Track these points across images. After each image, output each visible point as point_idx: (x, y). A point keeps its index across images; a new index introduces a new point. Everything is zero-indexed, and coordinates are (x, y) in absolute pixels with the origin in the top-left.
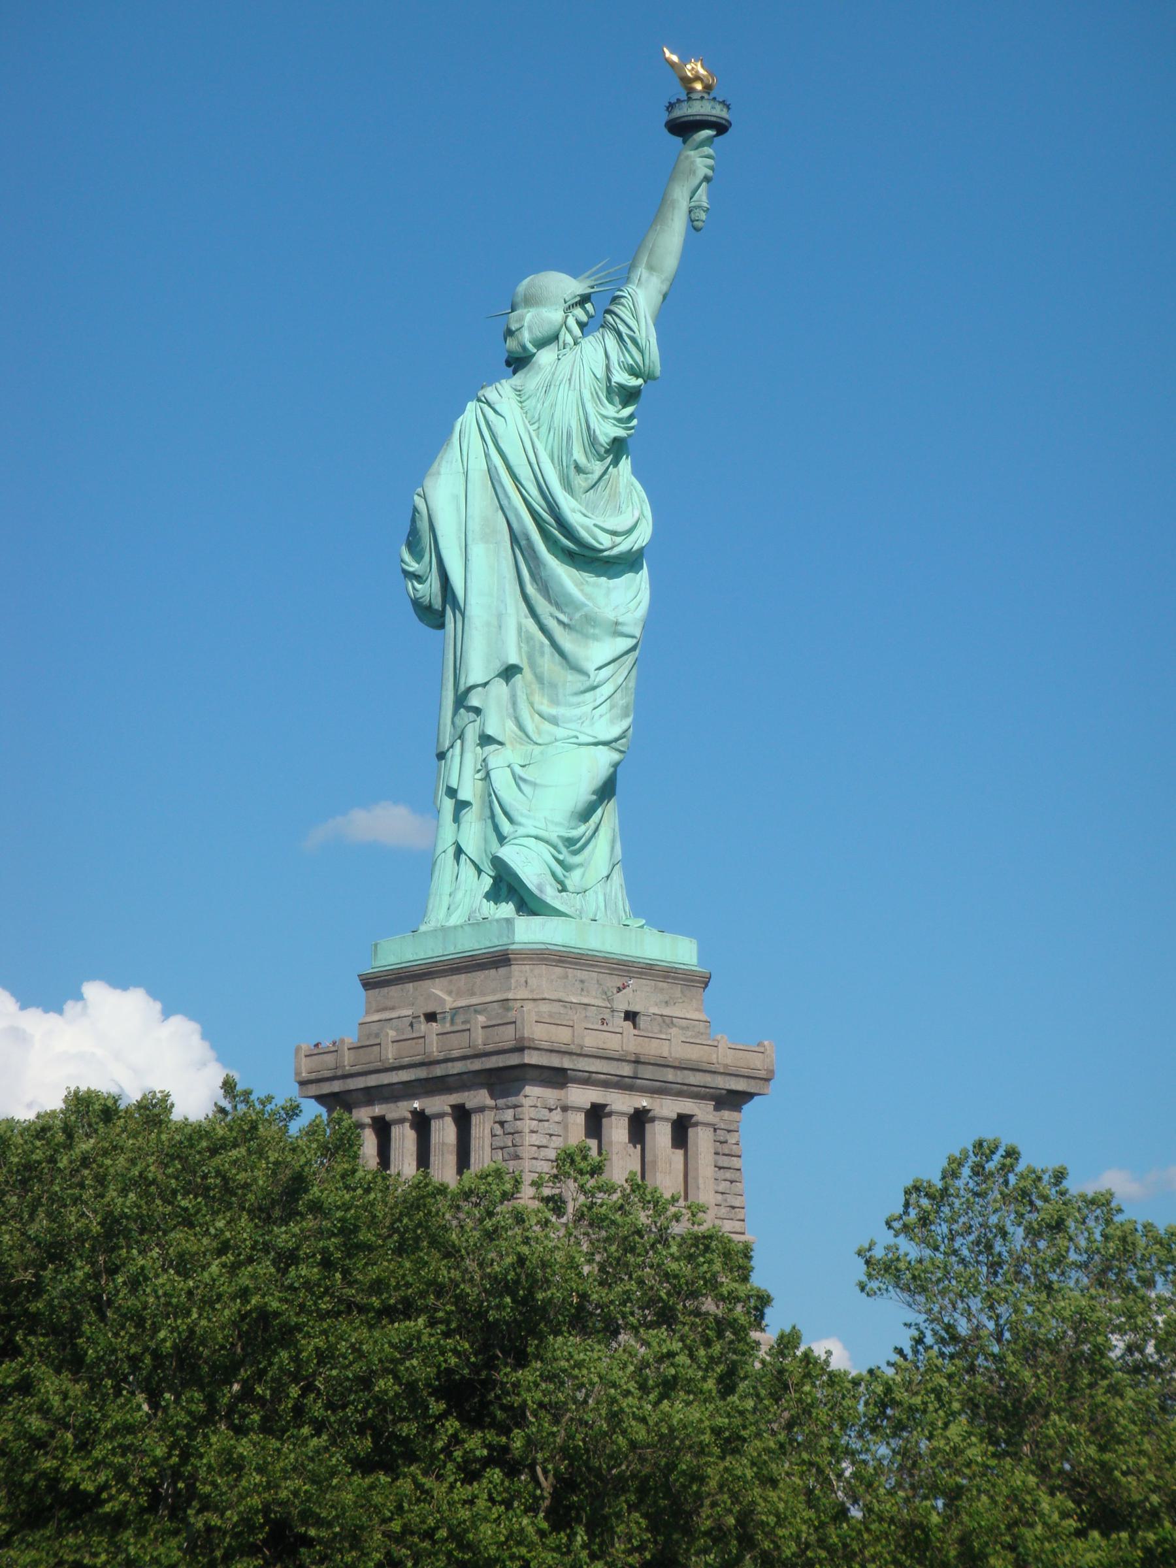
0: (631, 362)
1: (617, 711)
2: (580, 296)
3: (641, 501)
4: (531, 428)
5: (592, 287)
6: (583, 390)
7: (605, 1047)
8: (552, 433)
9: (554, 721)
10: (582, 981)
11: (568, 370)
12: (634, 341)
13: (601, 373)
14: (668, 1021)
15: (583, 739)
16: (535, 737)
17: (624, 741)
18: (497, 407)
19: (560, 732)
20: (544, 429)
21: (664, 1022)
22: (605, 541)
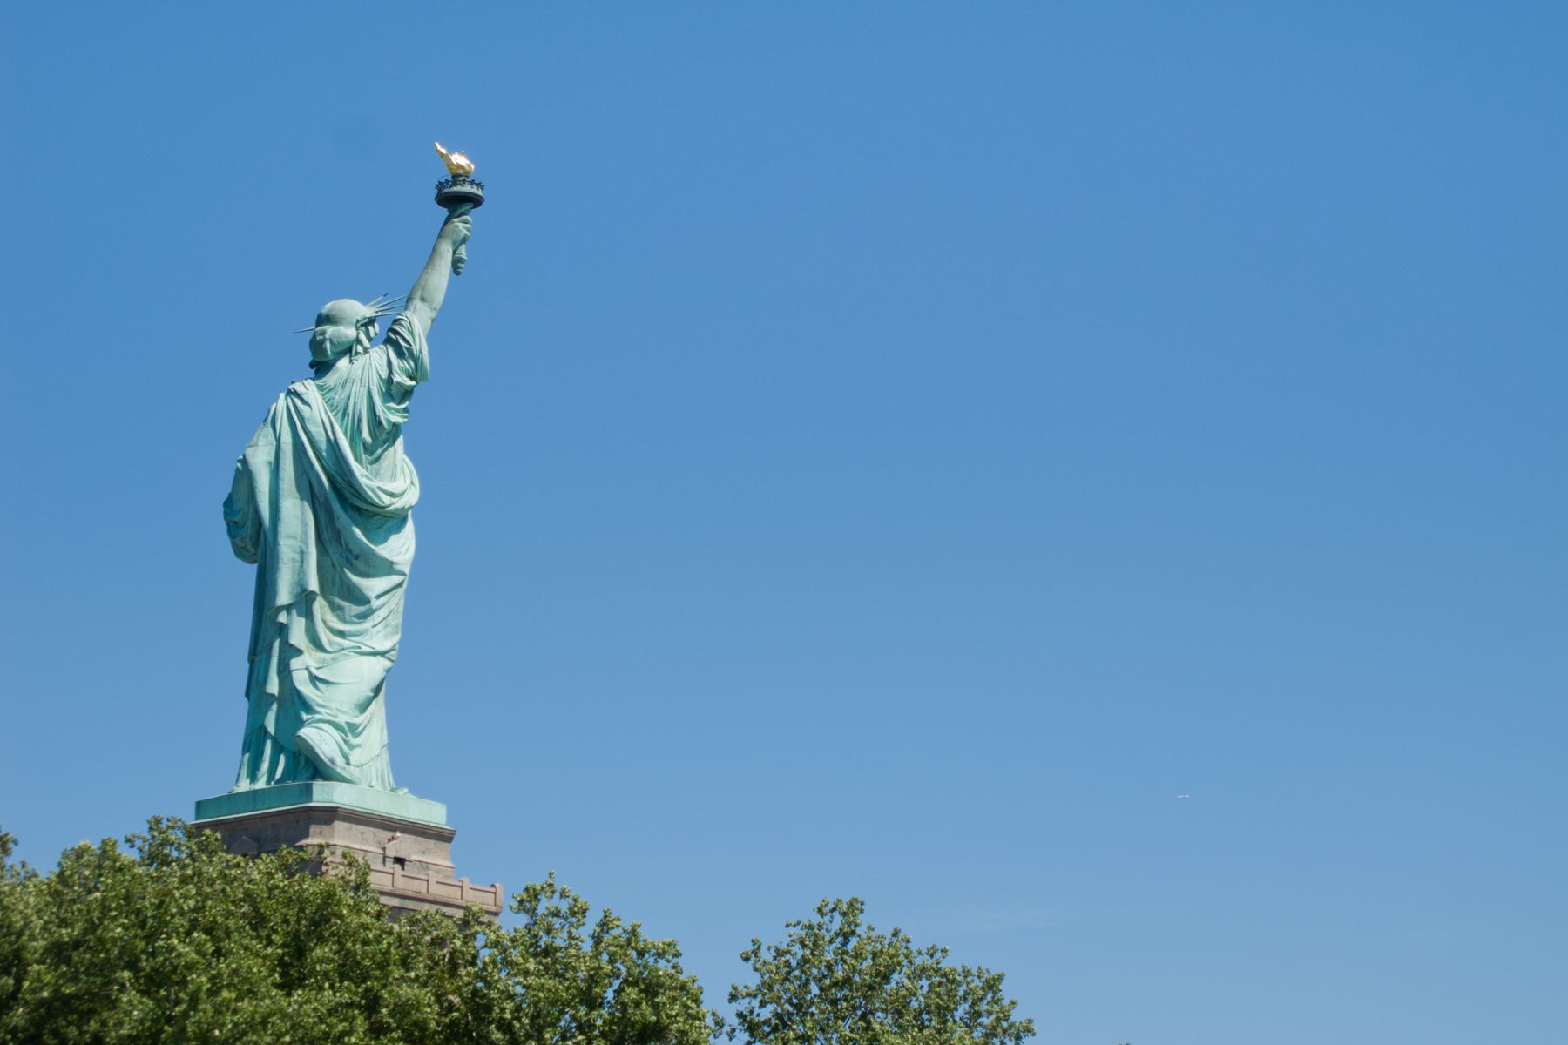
0: (408, 367)
1: (389, 629)
2: (368, 318)
3: (411, 472)
4: (331, 415)
5: (377, 312)
6: (371, 386)
7: (380, 883)
8: (346, 418)
9: (342, 634)
10: (362, 833)
11: (360, 372)
12: (410, 352)
13: (384, 375)
14: (424, 865)
15: (364, 649)
16: (327, 646)
17: (393, 652)
18: (305, 397)
19: (346, 643)
20: (340, 415)
21: (422, 866)
22: (387, 500)
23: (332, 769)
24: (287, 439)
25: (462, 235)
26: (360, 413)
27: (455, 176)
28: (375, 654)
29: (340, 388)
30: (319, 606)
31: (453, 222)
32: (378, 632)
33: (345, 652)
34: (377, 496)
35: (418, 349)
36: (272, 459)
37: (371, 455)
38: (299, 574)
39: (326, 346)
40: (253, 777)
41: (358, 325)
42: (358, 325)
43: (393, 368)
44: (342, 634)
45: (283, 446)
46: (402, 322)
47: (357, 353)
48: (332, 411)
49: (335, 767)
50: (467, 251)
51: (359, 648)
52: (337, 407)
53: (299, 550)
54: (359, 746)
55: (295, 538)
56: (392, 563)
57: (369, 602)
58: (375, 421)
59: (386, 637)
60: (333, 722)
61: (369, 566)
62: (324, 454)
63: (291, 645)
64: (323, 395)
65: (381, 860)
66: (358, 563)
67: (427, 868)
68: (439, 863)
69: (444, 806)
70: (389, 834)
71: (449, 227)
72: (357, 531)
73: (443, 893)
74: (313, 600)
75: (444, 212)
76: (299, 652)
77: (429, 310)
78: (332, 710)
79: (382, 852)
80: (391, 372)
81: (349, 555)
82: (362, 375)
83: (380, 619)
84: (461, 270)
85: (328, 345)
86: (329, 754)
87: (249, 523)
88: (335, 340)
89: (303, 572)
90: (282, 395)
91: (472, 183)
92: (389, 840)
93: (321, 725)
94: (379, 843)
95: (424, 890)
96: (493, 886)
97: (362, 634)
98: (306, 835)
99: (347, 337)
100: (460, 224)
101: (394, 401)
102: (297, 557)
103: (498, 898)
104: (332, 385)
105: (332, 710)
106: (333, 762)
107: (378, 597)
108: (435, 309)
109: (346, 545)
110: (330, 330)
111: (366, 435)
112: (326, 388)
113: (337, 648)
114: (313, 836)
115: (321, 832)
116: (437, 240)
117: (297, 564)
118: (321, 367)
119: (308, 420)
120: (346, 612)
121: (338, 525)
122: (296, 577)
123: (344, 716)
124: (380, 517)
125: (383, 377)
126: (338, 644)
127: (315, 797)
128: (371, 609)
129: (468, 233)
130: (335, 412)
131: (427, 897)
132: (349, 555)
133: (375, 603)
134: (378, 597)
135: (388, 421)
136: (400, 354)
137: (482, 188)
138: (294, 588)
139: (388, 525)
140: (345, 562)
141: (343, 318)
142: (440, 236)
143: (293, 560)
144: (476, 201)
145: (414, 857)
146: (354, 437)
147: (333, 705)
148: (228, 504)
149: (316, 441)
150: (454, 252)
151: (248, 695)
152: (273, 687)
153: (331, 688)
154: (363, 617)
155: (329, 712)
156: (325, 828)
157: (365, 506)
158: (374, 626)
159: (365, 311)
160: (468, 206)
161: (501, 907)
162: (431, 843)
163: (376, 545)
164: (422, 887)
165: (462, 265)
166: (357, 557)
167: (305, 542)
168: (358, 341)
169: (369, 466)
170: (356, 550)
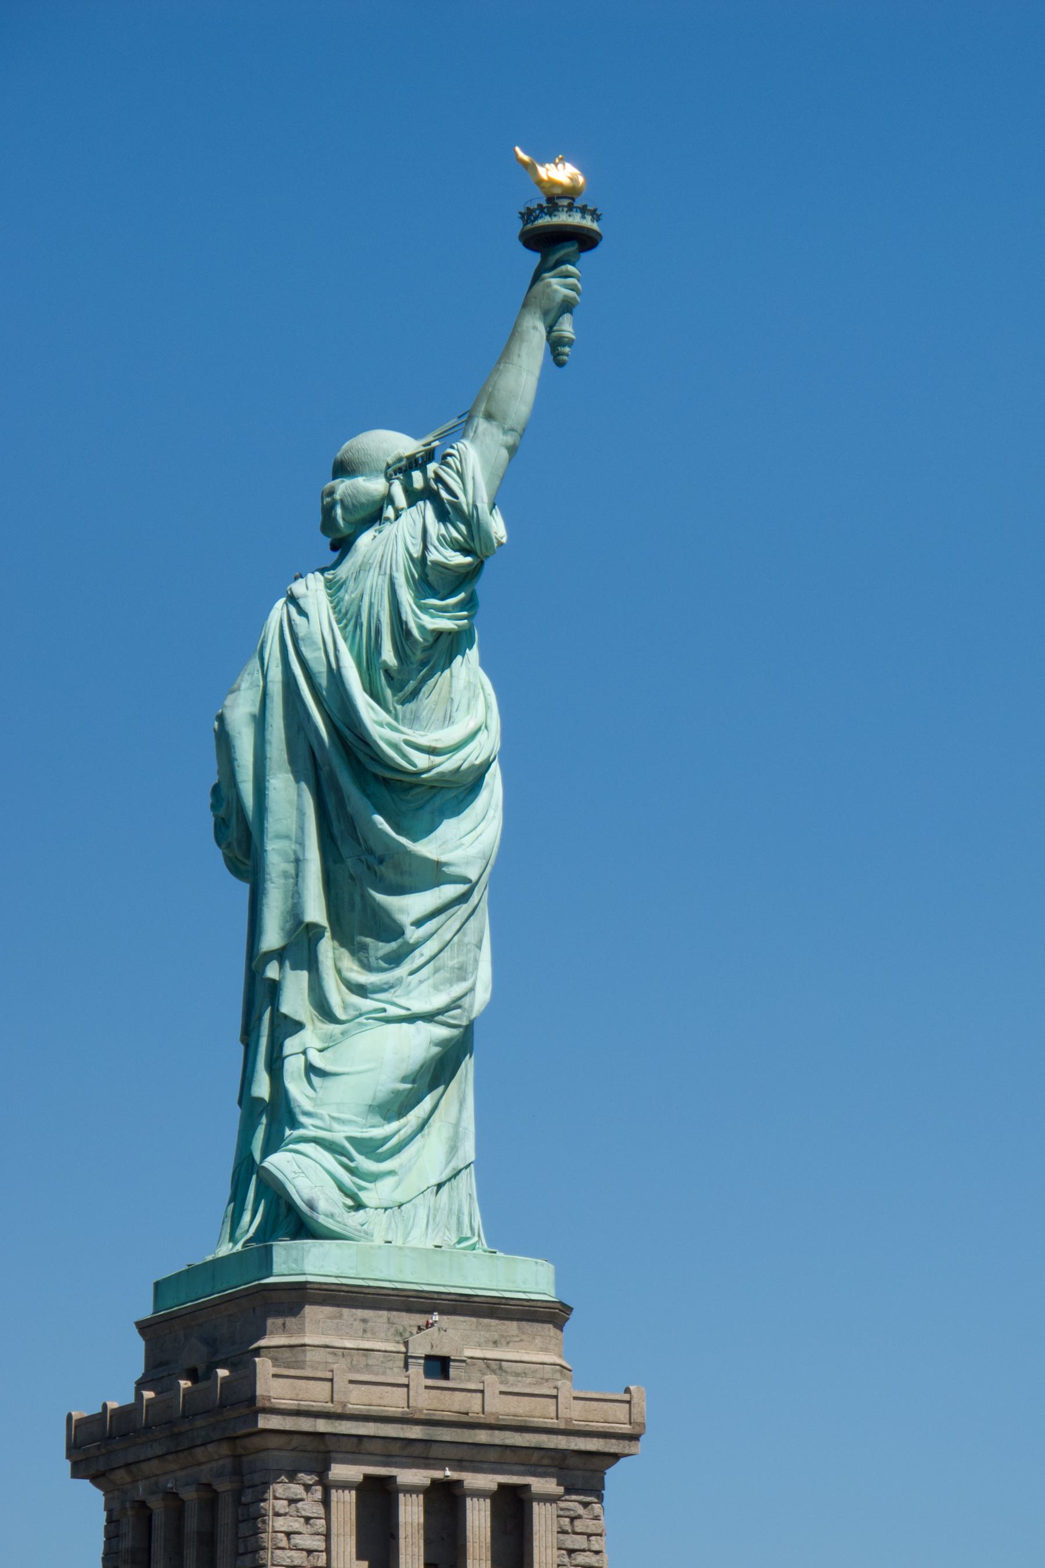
0: (455, 534)
2: (408, 458)
3: (488, 707)
6: (395, 574)
7: (382, 1402)
8: (358, 630)
9: (361, 990)
10: (364, 1321)
12: (457, 507)
13: (416, 553)
14: (496, 1366)
15: (393, 1011)
19: (367, 1004)
21: (488, 1367)
22: (422, 761)
23: (312, 1218)
24: (276, 674)
25: (559, 298)
26: (379, 620)
27: (551, 199)
28: (412, 1019)
29: (353, 580)
30: (327, 948)
31: (543, 279)
32: (421, 982)
33: (362, 1019)
34: (404, 756)
35: (471, 501)
36: (255, 709)
37: (401, 689)
38: (293, 897)
39: (336, 514)
40: (233, 1239)
41: (390, 471)
42: (390, 471)
43: (429, 539)
44: (361, 990)
45: (270, 685)
46: (449, 459)
47: (388, 519)
48: (339, 622)
49: (315, 1215)
50: (575, 327)
51: (384, 1010)
52: (346, 613)
53: (292, 857)
54: (392, 1173)
55: (287, 837)
56: (439, 865)
57: (402, 933)
58: (401, 631)
59: (436, 988)
60: (323, 1139)
61: (402, 873)
62: (324, 693)
63: (285, 1017)
64: (330, 595)
65: (402, 1364)
66: (382, 869)
67: (501, 1368)
68: (526, 1358)
69: (552, 1266)
70: (420, 1319)
71: (539, 286)
72: (379, 819)
73: (520, 1411)
74: (322, 936)
75: (534, 258)
76: (299, 1026)
77: (501, 431)
78: (322, 1119)
79: (403, 1349)
80: (425, 548)
81: (371, 859)
82: (383, 556)
83: (423, 960)
84: (565, 358)
85: (339, 511)
86: (307, 1194)
87: (234, 822)
88: (348, 501)
89: (299, 893)
90: (283, 600)
91: (583, 210)
92: (420, 1329)
93: (301, 1147)
94: (401, 1335)
95: (477, 1408)
96: (627, 1391)
97: (392, 987)
98: (262, 1333)
99: (375, 493)
100: (554, 281)
101: (434, 596)
102: (290, 868)
103: (634, 1410)
104: (344, 577)
105: (322, 1119)
106: (311, 1206)
107: (418, 923)
108: (512, 430)
109: (365, 841)
110: (343, 486)
111: (388, 655)
112: (339, 581)
113: (353, 1013)
114: (272, 1333)
115: (284, 1325)
116: (520, 312)
117: (292, 881)
118: (342, 545)
119: (303, 640)
120: (372, 952)
121: (349, 809)
122: (290, 901)
123: (346, 1128)
124: (417, 790)
125: (415, 555)
126: (355, 1008)
127: (276, 1269)
128: (406, 943)
129: (572, 294)
130: (345, 621)
131: (482, 1419)
132: (371, 859)
133: (412, 934)
134: (418, 923)
135: (422, 628)
136: (442, 515)
137: (596, 216)
138: (287, 921)
139: (438, 801)
140: (365, 869)
141: (363, 463)
142: (525, 305)
143: (285, 875)
144: (586, 240)
145: (468, 1352)
146: (369, 665)
147: (323, 1111)
148: (216, 790)
149: (314, 674)
150: (550, 330)
151: (240, 1103)
152: (262, 1088)
153: (330, 1082)
154: (395, 960)
155: (318, 1123)
156: (290, 1321)
157: (388, 775)
158: (412, 973)
159: (406, 445)
160: (571, 248)
161: (642, 1425)
162: (512, 1327)
163: (415, 840)
164: (473, 1404)
165: (567, 349)
166: (381, 861)
167: (301, 843)
168: (389, 499)
169: (399, 707)
170: (379, 851)
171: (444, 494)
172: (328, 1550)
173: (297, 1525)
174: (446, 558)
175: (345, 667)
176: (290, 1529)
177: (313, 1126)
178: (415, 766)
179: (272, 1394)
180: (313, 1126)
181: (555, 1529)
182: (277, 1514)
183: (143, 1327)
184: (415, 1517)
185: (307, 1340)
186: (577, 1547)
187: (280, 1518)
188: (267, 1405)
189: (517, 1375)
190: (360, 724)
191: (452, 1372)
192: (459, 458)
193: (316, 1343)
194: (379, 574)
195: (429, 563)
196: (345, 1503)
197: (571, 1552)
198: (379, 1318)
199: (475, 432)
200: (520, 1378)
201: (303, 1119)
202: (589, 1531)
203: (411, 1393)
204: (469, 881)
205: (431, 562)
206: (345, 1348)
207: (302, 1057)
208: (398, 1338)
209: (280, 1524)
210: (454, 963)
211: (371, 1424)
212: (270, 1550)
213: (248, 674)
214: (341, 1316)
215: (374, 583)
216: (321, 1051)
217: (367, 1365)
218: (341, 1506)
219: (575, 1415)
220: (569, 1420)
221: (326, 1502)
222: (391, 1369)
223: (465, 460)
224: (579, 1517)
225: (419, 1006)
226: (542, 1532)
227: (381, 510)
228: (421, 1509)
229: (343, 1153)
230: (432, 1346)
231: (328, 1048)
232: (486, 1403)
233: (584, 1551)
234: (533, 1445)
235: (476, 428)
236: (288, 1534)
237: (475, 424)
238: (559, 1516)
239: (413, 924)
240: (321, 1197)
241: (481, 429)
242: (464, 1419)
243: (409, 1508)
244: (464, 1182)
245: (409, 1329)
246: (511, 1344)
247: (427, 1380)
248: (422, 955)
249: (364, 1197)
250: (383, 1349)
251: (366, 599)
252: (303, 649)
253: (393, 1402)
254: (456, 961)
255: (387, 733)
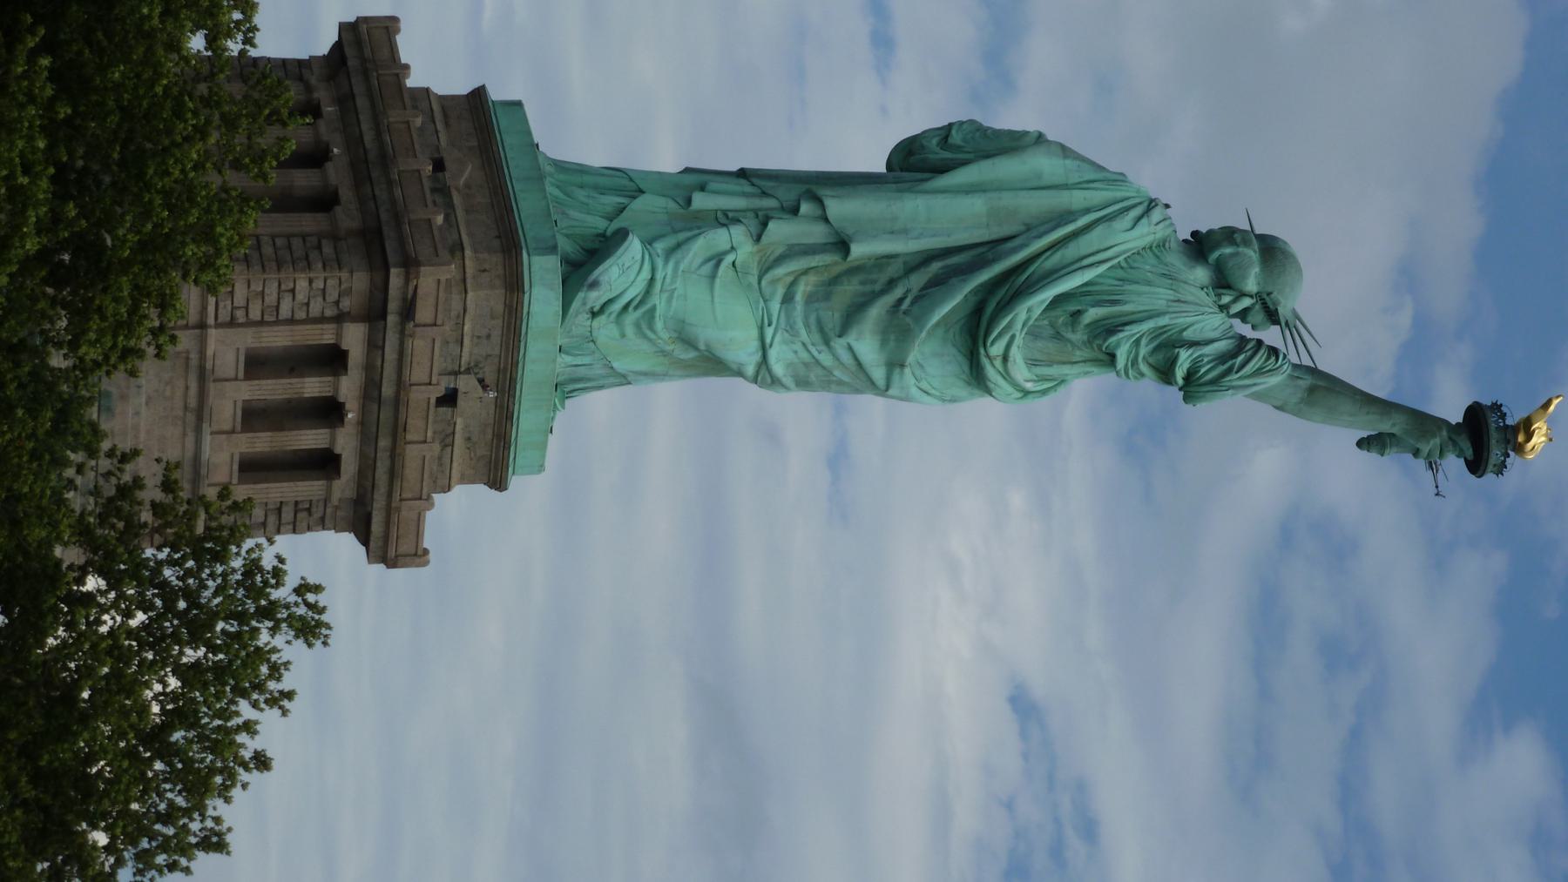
9: (788, 299)
10: (489, 336)
15: (769, 332)
19: (775, 306)
21: (447, 436)
22: (996, 349)
32: (796, 352)
33: (762, 303)
46: (1273, 358)
47: (1219, 296)
67: (446, 446)
68: (455, 464)
86: (604, 279)
93: (647, 266)
94: (476, 366)
107: (850, 348)
121: (954, 280)
125: (1185, 333)
126: (773, 294)
133: (839, 345)
135: (1118, 345)
136: (1223, 358)
155: (668, 280)
171: (1241, 358)
172: (277, 322)
173: (301, 297)
174: (1181, 365)
175: (1083, 274)
176: (297, 291)
177: (666, 275)
178: (993, 343)
179: (421, 279)
180: (666, 275)
181: (299, 499)
182: (311, 281)
183: (479, 94)
184: (309, 390)
185: (470, 295)
186: (283, 515)
187: (307, 284)
188: (411, 276)
189: (440, 458)
190: (1032, 293)
191: (442, 410)
192: (1278, 365)
193: (468, 302)
194: (1168, 300)
195: (1177, 350)
196: (325, 335)
197: (279, 511)
198: (494, 347)
199: (1298, 377)
200: (436, 461)
201: (671, 265)
202: (298, 523)
203: (423, 388)
204: (887, 390)
205: (1178, 352)
206: (463, 324)
207: (728, 247)
208: (472, 364)
209: (302, 284)
210: (813, 377)
211: (395, 356)
212: (277, 276)
213: (1079, 166)
214: (493, 317)
215: (1159, 296)
216: (734, 263)
217: (448, 342)
218: (319, 332)
219: (404, 513)
220: (399, 510)
221: (322, 319)
222: (445, 361)
223: (1272, 375)
224: (310, 514)
225: (773, 354)
226: (296, 489)
227: (1228, 287)
228: (317, 395)
229: (642, 302)
230: (465, 393)
231: (737, 272)
232: (415, 446)
233: (280, 520)
234: (376, 482)
235: (1301, 378)
236: (293, 291)
237: (1306, 377)
238: (311, 501)
239: (849, 344)
240: (601, 293)
241: (1301, 382)
242: (400, 429)
243: (318, 385)
244: (615, 381)
245: (481, 372)
246: (468, 451)
247: (435, 399)
248: (820, 353)
249: (602, 319)
250: (463, 354)
251: (1147, 289)
252: (1100, 227)
253: (418, 373)
254: (814, 379)
255: (1022, 316)
